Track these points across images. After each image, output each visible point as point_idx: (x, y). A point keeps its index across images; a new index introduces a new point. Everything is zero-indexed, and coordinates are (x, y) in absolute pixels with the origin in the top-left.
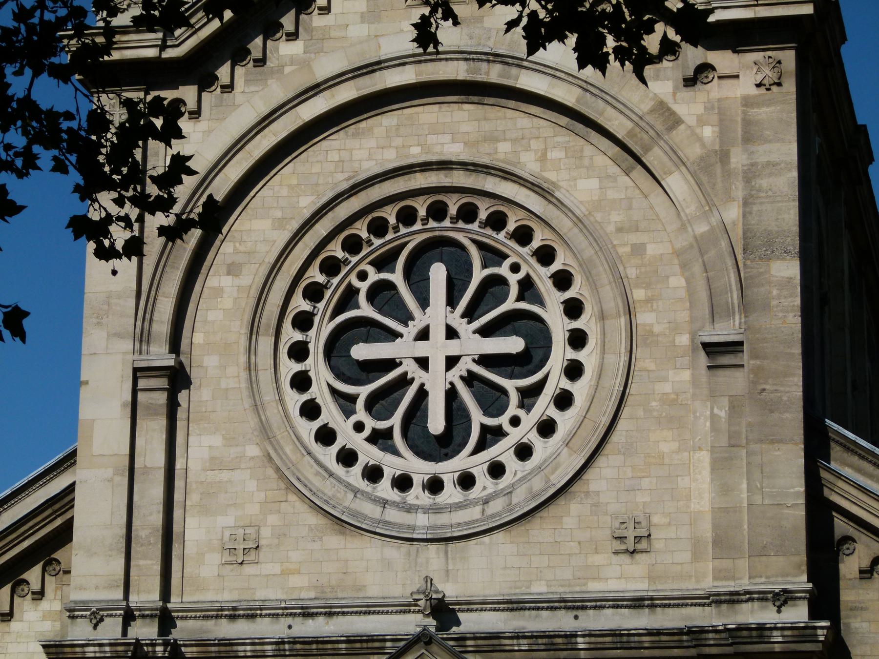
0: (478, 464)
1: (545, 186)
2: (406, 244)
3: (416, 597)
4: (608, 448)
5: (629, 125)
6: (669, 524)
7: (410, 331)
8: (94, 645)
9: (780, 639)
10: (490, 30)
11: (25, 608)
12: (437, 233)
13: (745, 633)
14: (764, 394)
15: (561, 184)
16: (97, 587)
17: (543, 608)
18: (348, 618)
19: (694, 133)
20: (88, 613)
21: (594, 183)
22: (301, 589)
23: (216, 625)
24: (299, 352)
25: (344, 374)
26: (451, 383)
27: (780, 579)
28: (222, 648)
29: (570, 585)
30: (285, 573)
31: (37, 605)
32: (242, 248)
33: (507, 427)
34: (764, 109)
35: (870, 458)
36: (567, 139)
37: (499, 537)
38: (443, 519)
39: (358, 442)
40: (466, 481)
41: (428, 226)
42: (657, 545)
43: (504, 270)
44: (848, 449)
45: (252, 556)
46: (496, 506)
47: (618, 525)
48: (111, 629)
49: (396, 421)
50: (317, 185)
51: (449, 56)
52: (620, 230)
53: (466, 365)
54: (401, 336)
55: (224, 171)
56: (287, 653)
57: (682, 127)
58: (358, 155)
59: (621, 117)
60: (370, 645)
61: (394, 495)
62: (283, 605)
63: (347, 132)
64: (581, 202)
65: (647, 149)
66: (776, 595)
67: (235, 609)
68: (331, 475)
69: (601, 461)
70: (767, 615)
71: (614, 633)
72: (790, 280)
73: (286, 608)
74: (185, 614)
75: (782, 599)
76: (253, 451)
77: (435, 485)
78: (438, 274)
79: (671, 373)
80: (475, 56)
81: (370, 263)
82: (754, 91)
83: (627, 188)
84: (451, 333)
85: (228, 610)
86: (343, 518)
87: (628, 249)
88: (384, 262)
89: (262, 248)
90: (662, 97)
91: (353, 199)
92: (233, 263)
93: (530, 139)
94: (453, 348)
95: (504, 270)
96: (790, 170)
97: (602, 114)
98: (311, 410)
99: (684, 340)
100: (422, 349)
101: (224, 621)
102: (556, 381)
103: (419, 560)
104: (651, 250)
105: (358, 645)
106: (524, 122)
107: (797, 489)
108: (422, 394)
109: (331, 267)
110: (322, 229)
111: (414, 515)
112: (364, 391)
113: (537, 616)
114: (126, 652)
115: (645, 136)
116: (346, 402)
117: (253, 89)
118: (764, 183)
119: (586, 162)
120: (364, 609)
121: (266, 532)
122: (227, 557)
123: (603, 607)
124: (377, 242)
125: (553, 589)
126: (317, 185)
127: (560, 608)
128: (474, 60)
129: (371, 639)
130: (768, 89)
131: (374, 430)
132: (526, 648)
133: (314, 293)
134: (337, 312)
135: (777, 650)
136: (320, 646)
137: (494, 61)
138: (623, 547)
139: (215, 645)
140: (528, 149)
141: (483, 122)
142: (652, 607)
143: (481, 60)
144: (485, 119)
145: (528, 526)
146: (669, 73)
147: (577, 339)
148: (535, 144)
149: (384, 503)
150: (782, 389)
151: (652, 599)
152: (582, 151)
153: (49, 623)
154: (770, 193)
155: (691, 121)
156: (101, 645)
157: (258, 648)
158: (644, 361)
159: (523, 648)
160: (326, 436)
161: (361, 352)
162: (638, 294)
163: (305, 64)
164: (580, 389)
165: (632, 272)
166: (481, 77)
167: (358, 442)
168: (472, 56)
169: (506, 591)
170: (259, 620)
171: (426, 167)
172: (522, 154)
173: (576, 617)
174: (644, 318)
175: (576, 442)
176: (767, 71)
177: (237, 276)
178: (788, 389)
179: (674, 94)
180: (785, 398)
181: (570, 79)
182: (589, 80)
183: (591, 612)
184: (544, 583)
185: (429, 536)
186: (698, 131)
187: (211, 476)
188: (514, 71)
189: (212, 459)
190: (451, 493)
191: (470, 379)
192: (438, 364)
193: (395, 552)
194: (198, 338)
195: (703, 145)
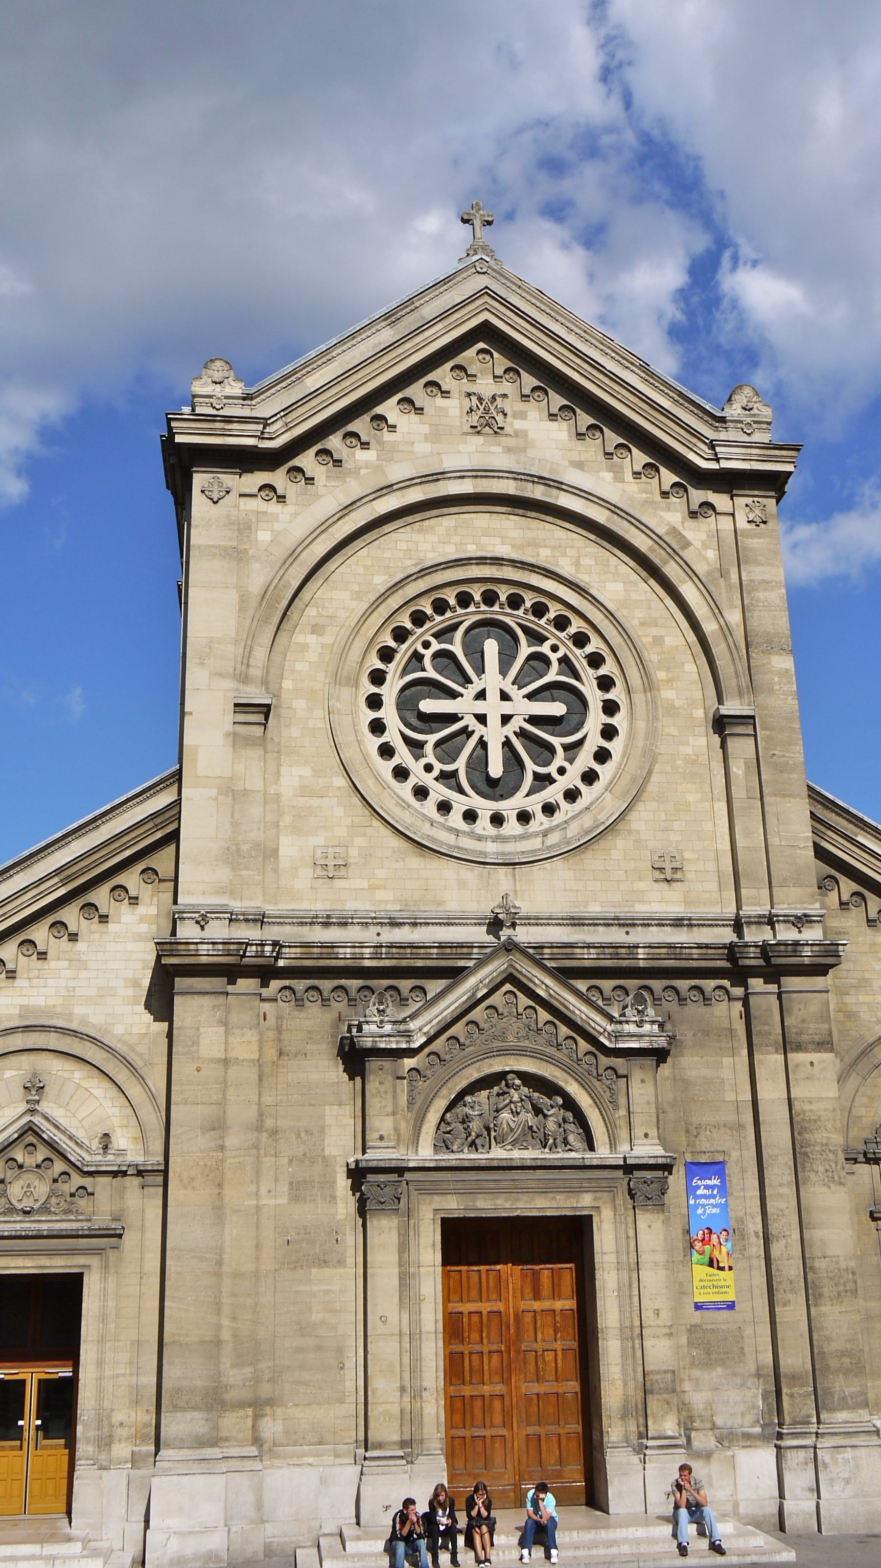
0: (534, 804)
1: (582, 584)
2: (461, 622)
3: (496, 911)
4: (645, 796)
5: (650, 542)
6: (698, 859)
7: (470, 691)
8: (208, 943)
9: (809, 954)
10: (534, 459)
11: (123, 911)
12: (488, 616)
13: (782, 948)
14: (774, 758)
15: (593, 584)
16: (204, 893)
17: (597, 925)
18: (431, 928)
19: (700, 554)
20: (197, 915)
21: (619, 586)
22: (387, 902)
23: (311, 930)
24: (374, 702)
25: (411, 724)
26: (506, 737)
27: (799, 906)
28: (325, 950)
29: (620, 907)
30: (373, 888)
31: (134, 909)
32: (324, 613)
33: (555, 775)
34: (756, 540)
35: (845, 815)
36: (596, 550)
37: (558, 863)
38: (509, 847)
39: (428, 779)
40: (524, 817)
41: (481, 609)
42: (690, 876)
43: (545, 649)
44: (827, 808)
45: (342, 872)
46: (553, 838)
47: (656, 858)
48: (218, 930)
49: (460, 764)
50: (389, 567)
51: (501, 474)
52: (642, 624)
53: (517, 723)
54: (462, 695)
55: (311, 547)
56: (383, 956)
57: (692, 548)
58: (423, 546)
59: (643, 535)
60: (459, 950)
61: (462, 825)
62: (374, 915)
63: (413, 528)
64: (610, 600)
65: (665, 563)
66: (796, 917)
67: (328, 917)
68: (409, 806)
69: (640, 806)
70: (787, 934)
71: (670, 946)
72: (787, 671)
73: (375, 918)
74: (282, 920)
75: (801, 921)
76: (341, 781)
77: (497, 820)
78: (491, 648)
79: (691, 739)
80: (523, 477)
81: (433, 635)
82: (748, 526)
83: (646, 593)
84: (505, 696)
85: (323, 918)
86: (424, 842)
87: (650, 639)
88: (443, 634)
89: (342, 614)
90: (673, 523)
91: (420, 581)
92: (316, 625)
93: (566, 548)
94: (507, 708)
95: (545, 649)
96: (780, 588)
97: (627, 532)
98: (386, 751)
99: (700, 713)
100: (480, 707)
101: (318, 928)
102: (595, 741)
103: (491, 881)
104: (669, 641)
105: (448, 951)
106: (560, 534)
107: (806, 834)
108: (482, 744)
109: (401, 635)
110: (394, 602)
111: (484, 843)
112: (432, 739)
113: (594, 931)
114: (239, 950)
115: (663, 553)
116: (416, 747)
117: (333, 483)
118: (761, 595)
119: (612, 569)
120: (445, 921)
121: (354, 852)
122: (319, 872)
123: (649, 925)
124: (438, 618)
125: (606, 909)
126: (389, 567)
127: (612, 925)
128: (521, 479)
129: (461, 946)
130: (758, 526)
131: (441, 771)
132: (595, 957)
133: (386, 655)
134: (405, 672)
135: (806, 963)
136: (414, 951)
137: (538, 483)
138: (663, 876)
139: (318, 947)
140: (564, 555)
141: (526, 531)
142: (690, 926)
143: (528, 481)
144: (529, 529)
145: (582, 857)
146: (678, 507)
147: (610, 708)
148: (569, 552)
149: (457, 832)
150: (788, 755)
151: (690, 919)
152: (608, 561)
153: (146, 925)
154: (766, 604)
155: (697, 544)
156: (213, 943)
157: (357, 950)
158: (669, 727)
159: (592, 956)
160: (401, 773)
161: (428, 706)
162: (661, 675)
163: (378, 469)
164: (615, 746)
165: (654, 658)
166: (527, 494)
167: (428, 779)
168: (520, 477)
169: (566, 910)
170: (350, 927)
171: (481, 561)
172: (560, 558)
173: (627, 933)
174: (667, 694)
175: (618, 790)
176: (757, 512)
177: (321, 635)
178: (792, 755)
179: (683, 523)
180: (791, 762)
181: (601, 502)
182: (619, 505)
183: (640, 928)
184: (598, 903)
185: (500, 861)
186: (703, 552)
187: (302, 801)
188: (555, 492)
189: (302, 787)
190: (512, 826)
191: (522, 734)
192: (494, 720)
193: (470, 874)
194: (287, 684)
195: (709, 564)
